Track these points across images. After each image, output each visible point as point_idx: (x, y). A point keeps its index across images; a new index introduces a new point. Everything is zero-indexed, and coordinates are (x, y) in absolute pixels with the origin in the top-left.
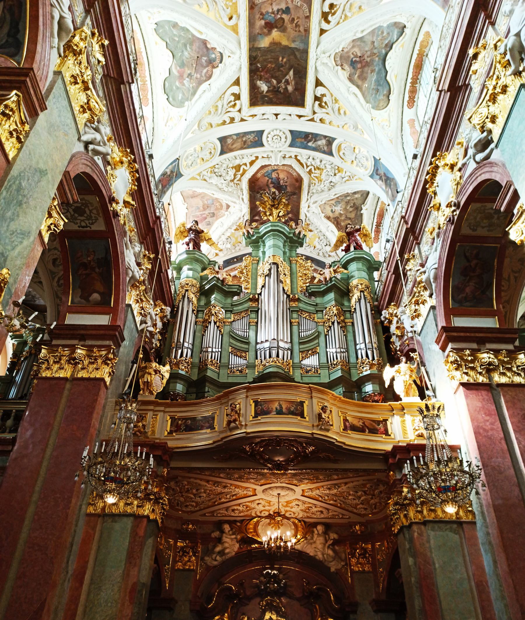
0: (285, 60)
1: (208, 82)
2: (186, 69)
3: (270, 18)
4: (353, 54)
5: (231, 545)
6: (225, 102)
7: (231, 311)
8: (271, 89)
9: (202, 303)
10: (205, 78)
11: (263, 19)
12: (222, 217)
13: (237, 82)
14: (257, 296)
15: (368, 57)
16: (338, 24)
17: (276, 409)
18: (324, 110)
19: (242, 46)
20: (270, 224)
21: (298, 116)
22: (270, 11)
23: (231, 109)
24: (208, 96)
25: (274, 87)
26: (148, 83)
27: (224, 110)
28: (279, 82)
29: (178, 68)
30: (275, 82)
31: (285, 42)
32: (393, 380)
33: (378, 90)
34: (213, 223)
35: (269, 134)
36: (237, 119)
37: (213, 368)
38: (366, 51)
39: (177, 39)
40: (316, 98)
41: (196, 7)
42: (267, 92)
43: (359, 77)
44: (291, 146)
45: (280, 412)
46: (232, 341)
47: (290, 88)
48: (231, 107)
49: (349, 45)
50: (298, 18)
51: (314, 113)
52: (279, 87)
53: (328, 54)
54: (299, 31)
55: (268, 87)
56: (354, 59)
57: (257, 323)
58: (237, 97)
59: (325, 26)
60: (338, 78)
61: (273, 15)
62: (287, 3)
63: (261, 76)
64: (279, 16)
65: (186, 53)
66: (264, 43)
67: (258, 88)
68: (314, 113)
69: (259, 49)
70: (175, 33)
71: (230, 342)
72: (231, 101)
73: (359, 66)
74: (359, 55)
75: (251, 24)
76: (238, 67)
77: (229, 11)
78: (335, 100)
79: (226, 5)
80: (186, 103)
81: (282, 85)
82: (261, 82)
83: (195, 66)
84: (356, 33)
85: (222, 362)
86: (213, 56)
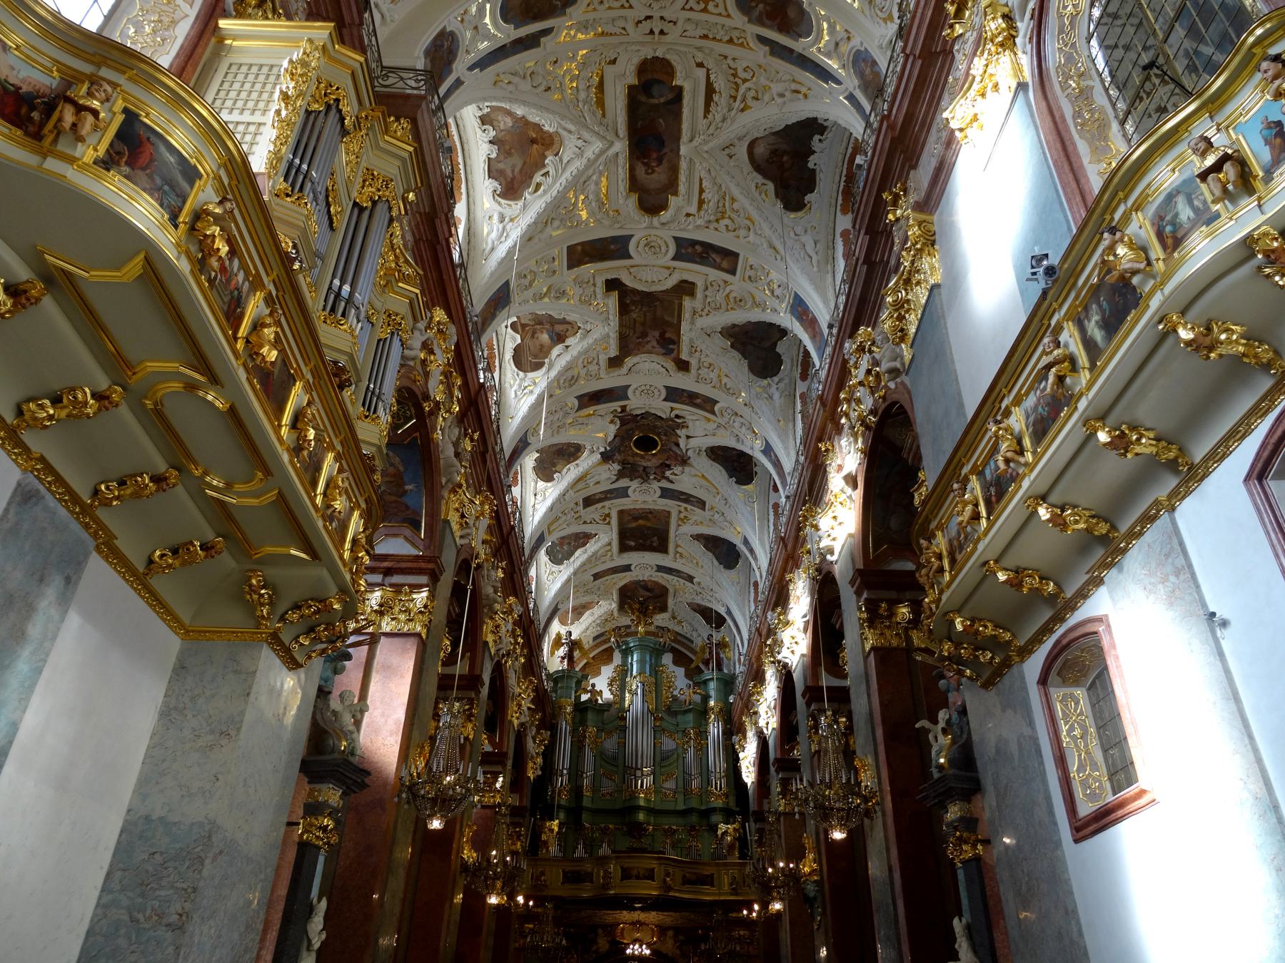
5: (603, 944)
45: (638, 878)
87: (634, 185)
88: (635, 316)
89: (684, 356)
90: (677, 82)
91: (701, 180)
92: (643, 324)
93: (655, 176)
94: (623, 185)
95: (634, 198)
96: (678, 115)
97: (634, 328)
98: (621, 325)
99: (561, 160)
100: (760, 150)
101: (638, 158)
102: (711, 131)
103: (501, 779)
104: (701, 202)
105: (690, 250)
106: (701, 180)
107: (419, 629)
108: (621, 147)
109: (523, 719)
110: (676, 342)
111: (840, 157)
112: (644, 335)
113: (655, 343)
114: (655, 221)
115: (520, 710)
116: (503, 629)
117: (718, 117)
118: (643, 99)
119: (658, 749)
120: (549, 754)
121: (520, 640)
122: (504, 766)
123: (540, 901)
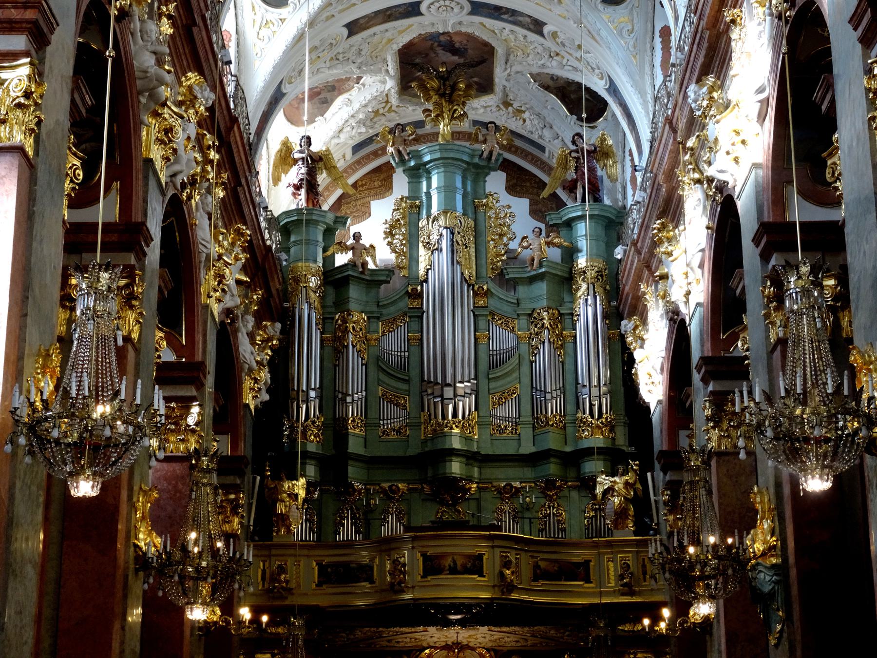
7: (378, 318)
9: (330, 301)
12: (349, 90)
14: (419, 288)
17: (450, 566)
20: (437, 147)
32: (606, 492)
34: (332, 101)
35: (432, 4)
37: (357, 431)
44: (472, 13)
45: (454, 571)
46: (382, 377)
57: (421, 340)
71: (379, 379)
85: (369, 416)
103: (195, 410)
107: (18, 138)
109: (229, 302)
115: (223, 284)
116: (180, 136)
119: (482, 348)
120: (281, 363)
121: (213, 155)
122: (200, 386)
123: (280, 616)
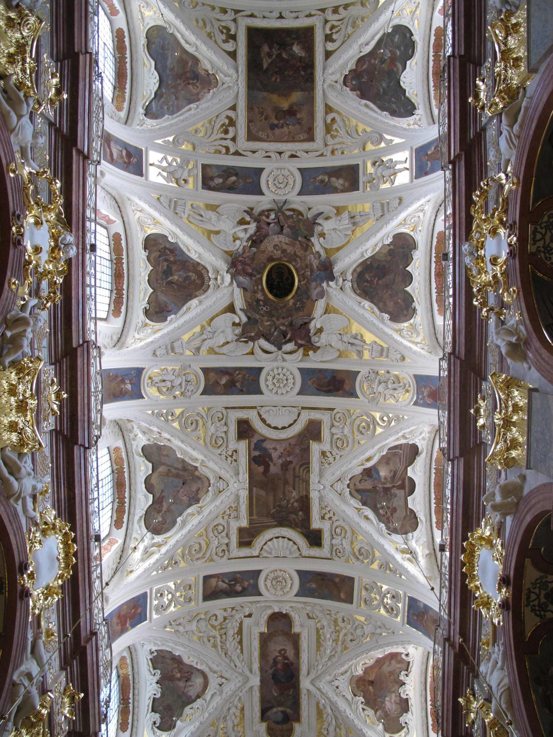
0: (273, 79)
1: (362, 54)
2: (386, 69)
3: (290, 120)
4: (198, 87)
6: (343, 32)
8: (288, 48)
10: (366, 58)
11: (299, 119)
13: (328, 54)
15: (180, 84)
16: (218, 116)
18: (224, 24)
19: (321, 91)
21: (255, 17)
22: (290, 127)
23: (336, 23)
24: (363, 39)
25: (284, 49)
26: (431, 54)
27: (345, 23)
28: (279, 56)
29: (395, 70)
30: (284, 56)
31: (274, 97)
33: (163, 48)
36: (329, 12)
38: (182, 90)
39: (393, 99)
40: (234, 37)
41: (368, 129)
42: (293, 44)
43: (188, 63)
47: (266, 48)
48: (337, 27)
49: (203, 96)
50: (261, 121)
51: (235, 20)
52: (279, 49)
53: (225, 86)
54: (258, 108)
55: (291, 49)
56: (195, 81)
58: (328, 38)
59: (231, 114)
60: (211, 62)
61: (288, 122)
62: (273, 134)
63: (301, 61)
64: (281, 122)
65: (384, 85)
66: (296, 96)
67: (303, 48)
68: (235, 20)
69: (302, 90)
70: (394, 106)
72: (337, 32)
73: (188, 75)
74: (190, 86)
75: (312, 115)
76: (326, 71)
77: (335, 127)
78: (211, 38)
79: (338, 132)
80: (390, 30)
81: (275, 52)
82: (300, 55)
83: (376, 72)
84: (197, 107)
86: (354, 82)
87: (295, 640)
88: (294, 494)
89: (243, 446)
90: (264, 725)
91: (242, 652)
92: (286, 482)
93: (279, 648)
94: (304, 644)
95: (296, 629)
96: (263, 700)
97: (295, 476)
98: (307, 482)
99: (352, 673)
100: (198, 681)
101: (292, 664)
102: (237, 698)
104: (240, 632)
105: (246, 584)
106: (242, 652)
108: (305, 684)
110: (254, 460)
111: (136, 681)
112: (285, 466)
113: (275, 455)
114: (277, 610)
117: (233, 710)
118: (289, 711)
